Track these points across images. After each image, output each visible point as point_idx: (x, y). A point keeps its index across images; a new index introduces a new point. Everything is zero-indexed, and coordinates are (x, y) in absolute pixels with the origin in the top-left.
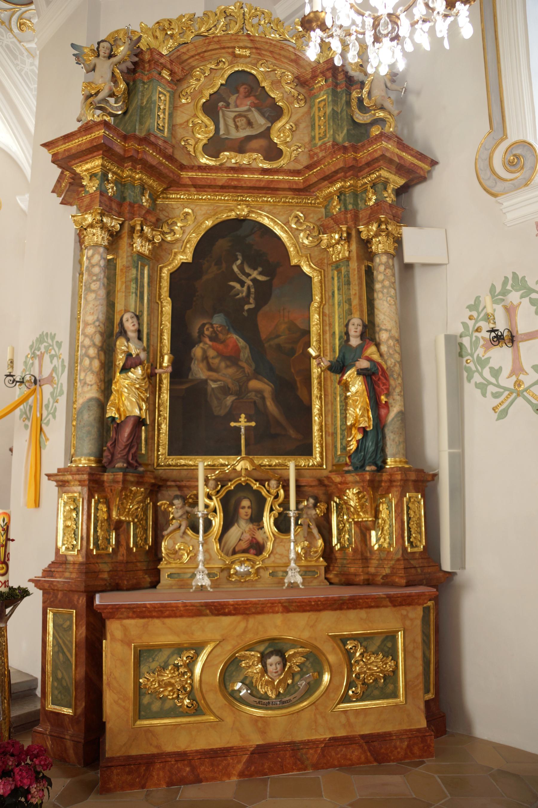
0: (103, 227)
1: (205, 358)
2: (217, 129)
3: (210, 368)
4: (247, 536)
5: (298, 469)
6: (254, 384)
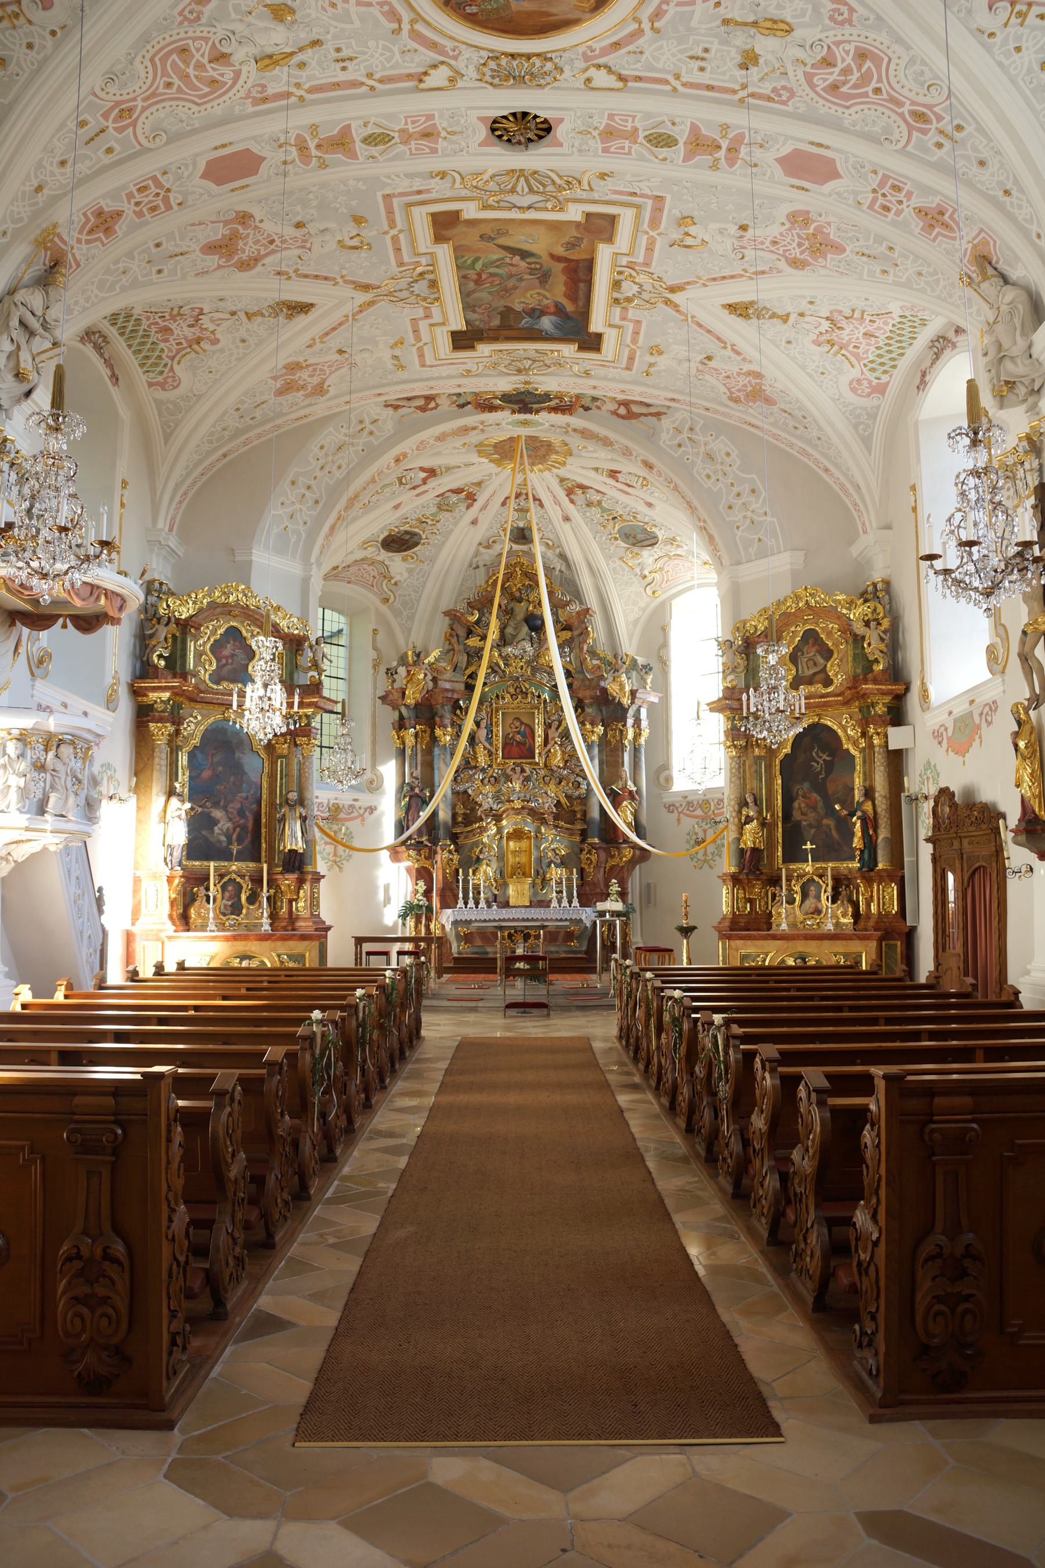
0: (735, 746)
1: (800, 808)
2: (797, 671)
3: (802, 814)
4: (813, 906)
5: (833, 869)
6: (825, 821)
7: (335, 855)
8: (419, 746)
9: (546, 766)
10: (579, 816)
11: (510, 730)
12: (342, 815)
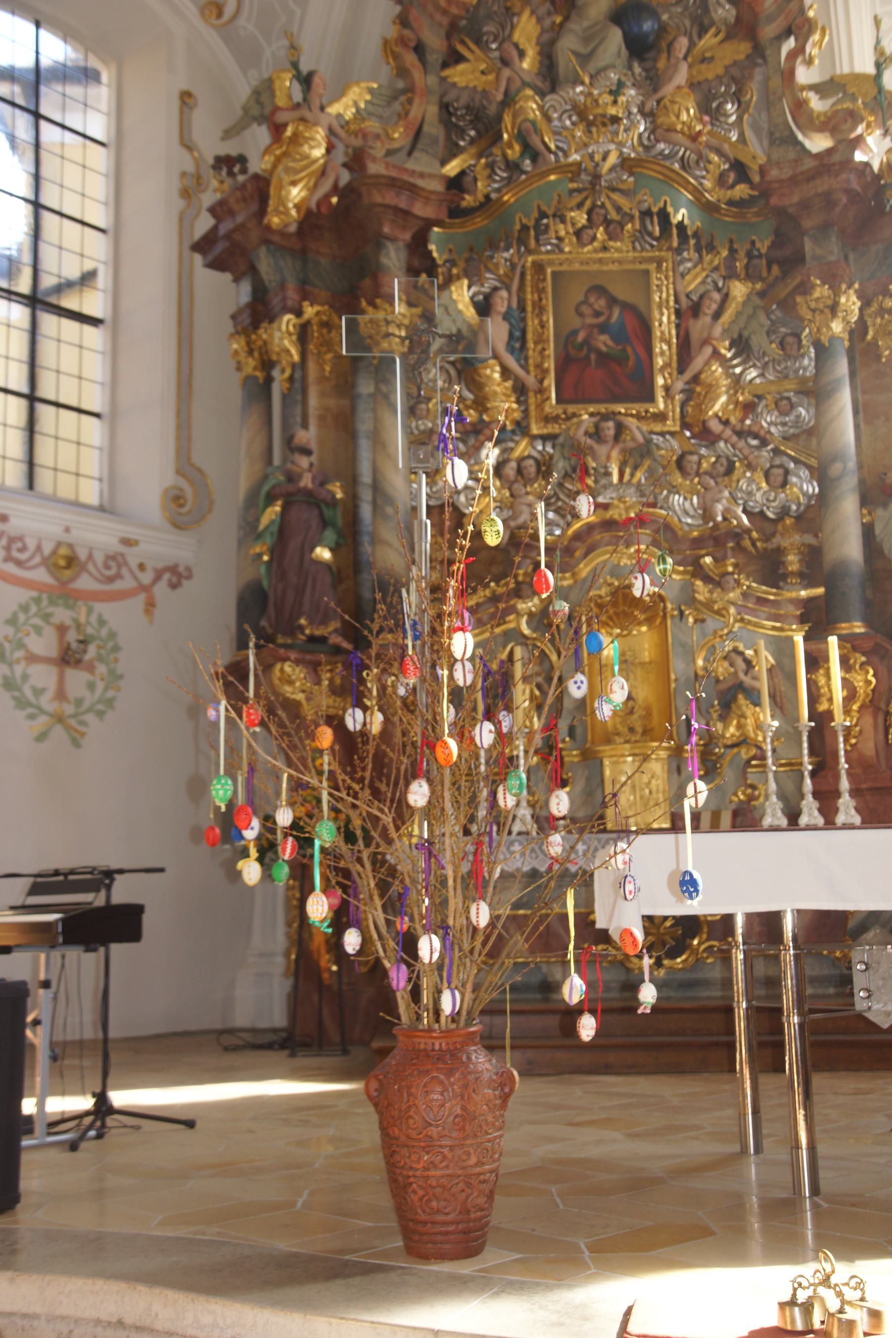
7: (61, 695)
8: (312, 366)
9: (685, 425)
10: (793, 562)
11: (577, 322)
12: (85, 583)
